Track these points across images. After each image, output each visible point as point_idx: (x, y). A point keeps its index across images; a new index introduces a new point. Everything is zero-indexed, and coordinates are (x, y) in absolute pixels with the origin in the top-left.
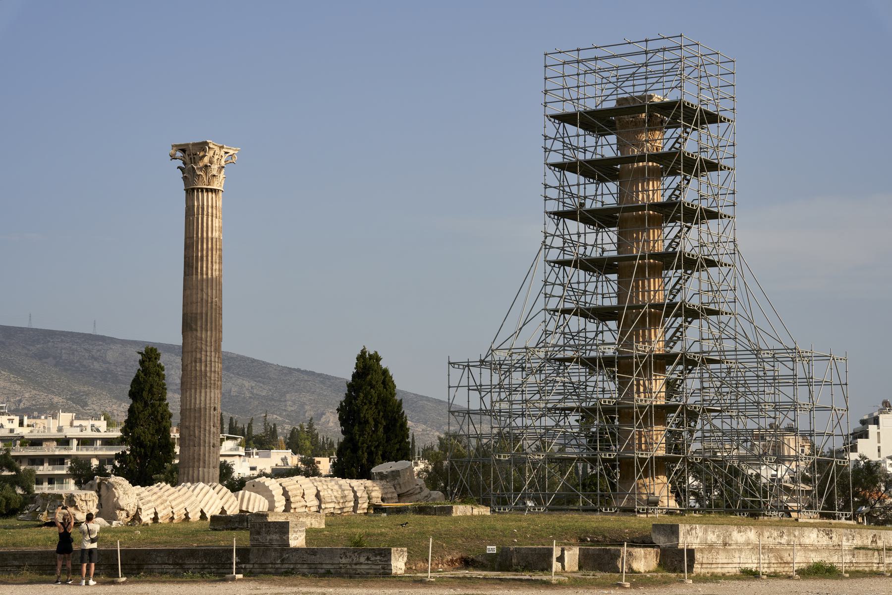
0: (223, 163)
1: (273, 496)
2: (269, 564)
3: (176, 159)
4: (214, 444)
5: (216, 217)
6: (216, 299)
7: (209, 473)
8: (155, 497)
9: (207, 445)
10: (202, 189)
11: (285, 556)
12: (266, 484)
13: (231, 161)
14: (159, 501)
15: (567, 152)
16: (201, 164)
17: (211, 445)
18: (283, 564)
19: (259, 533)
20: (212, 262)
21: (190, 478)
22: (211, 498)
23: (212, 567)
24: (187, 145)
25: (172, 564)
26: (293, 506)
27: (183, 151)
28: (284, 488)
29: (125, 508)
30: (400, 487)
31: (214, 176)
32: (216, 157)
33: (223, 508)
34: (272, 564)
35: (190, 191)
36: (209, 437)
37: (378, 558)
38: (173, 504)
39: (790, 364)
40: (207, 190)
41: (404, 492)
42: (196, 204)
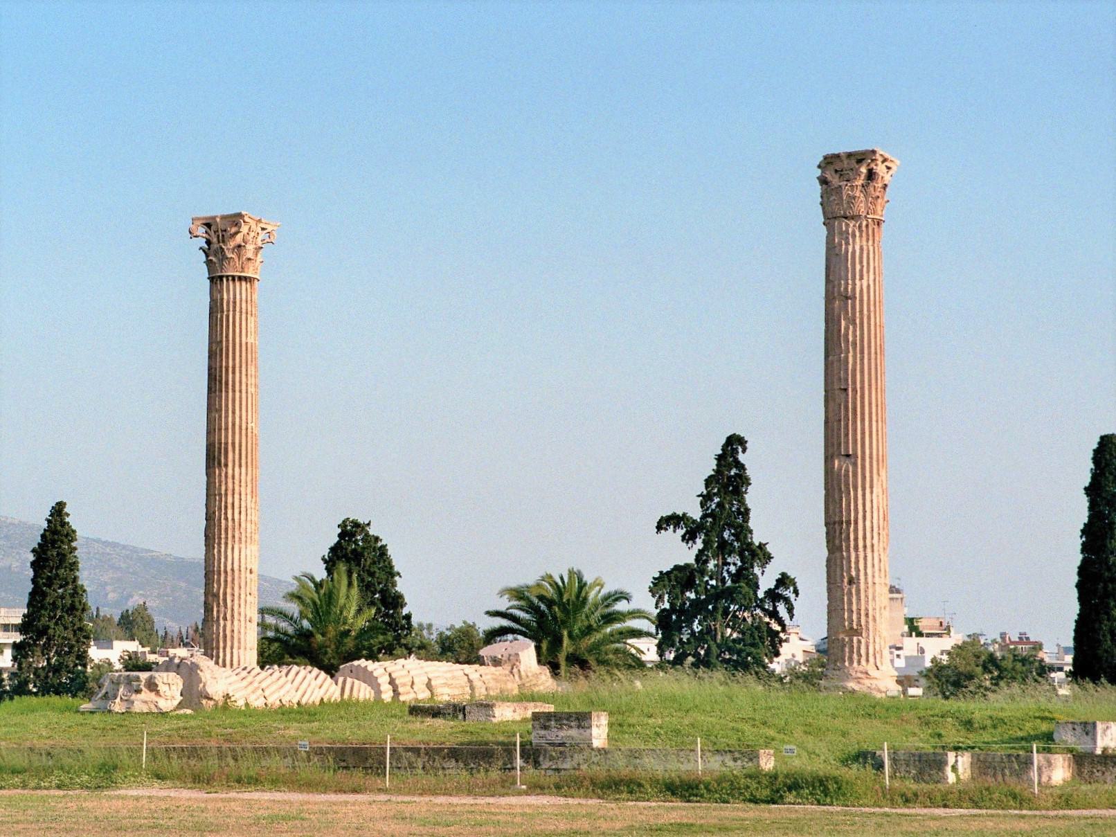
1: (379, 685)
4: (251, 618)
5: (252, 315)
6: (253, 424)
8: (245, 683)
9: (242, 619)
10: (233, 278)
12: (370, 669)
13: (269, 241)
14: (251, 688)
16: (232, 244)
17: (248, 619)
20: (247, 375)
21: (221, 661)
22: (309, 685)
24: (214, 218)
27: (208, 225)
28: (390, 675)
31: (249, 259)
32: (252, 234)
35: (215, 280)
38: (267, 693)
40: (240, 278)
42: (225, 297)
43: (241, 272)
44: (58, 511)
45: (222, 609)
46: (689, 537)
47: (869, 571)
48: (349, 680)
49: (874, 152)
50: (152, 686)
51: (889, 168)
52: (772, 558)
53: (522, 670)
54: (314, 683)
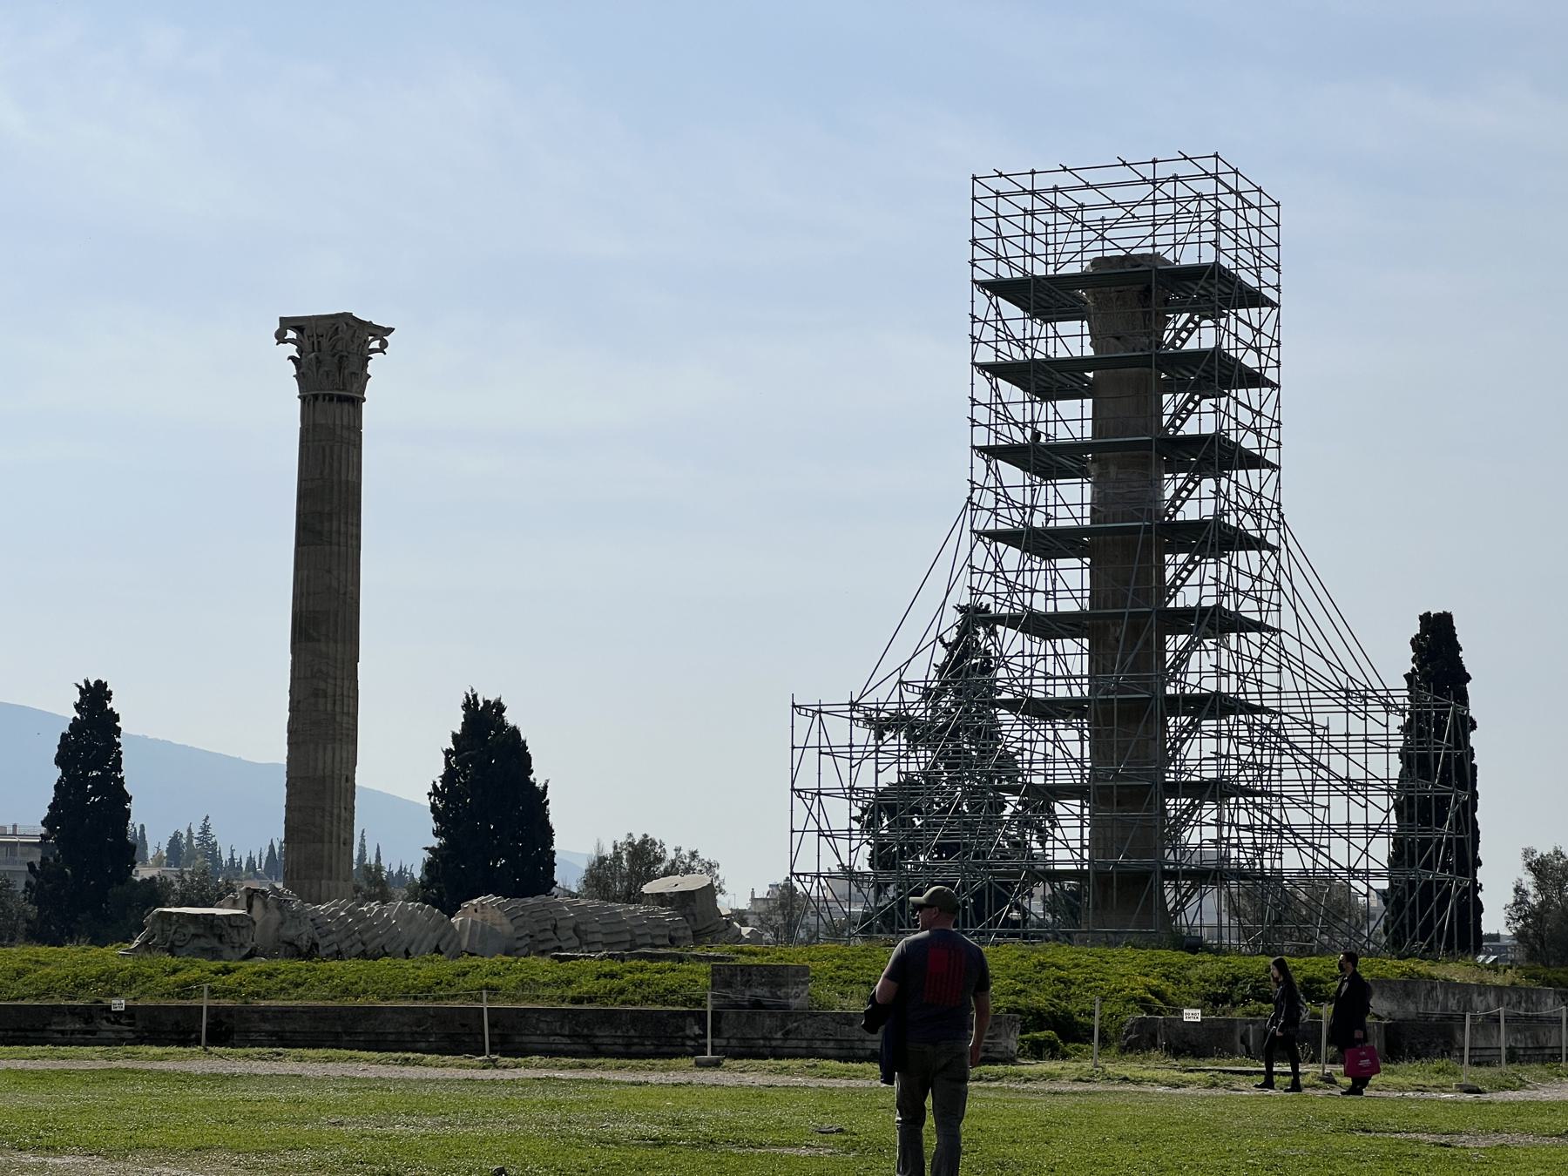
2: (759, 1039)
3: (285, 342)
4: (345, 839)
7: (337, 889)
11: (792, 1025)
15: (1003, 346)
18: (786, 1039)
19: (729, 985)
20: (346, 523)
23: (646, 1043)
25: (569, 1036)
29: (296, 943)
30: (695, 920)
33: (438, 946)
34: (764, 1038)
36: (339, 827)
39: (1382, 717)
40: (341, 399)
41: (700, 928)
43: (343, 390)
44: (95, 697)
46: (914, 742)
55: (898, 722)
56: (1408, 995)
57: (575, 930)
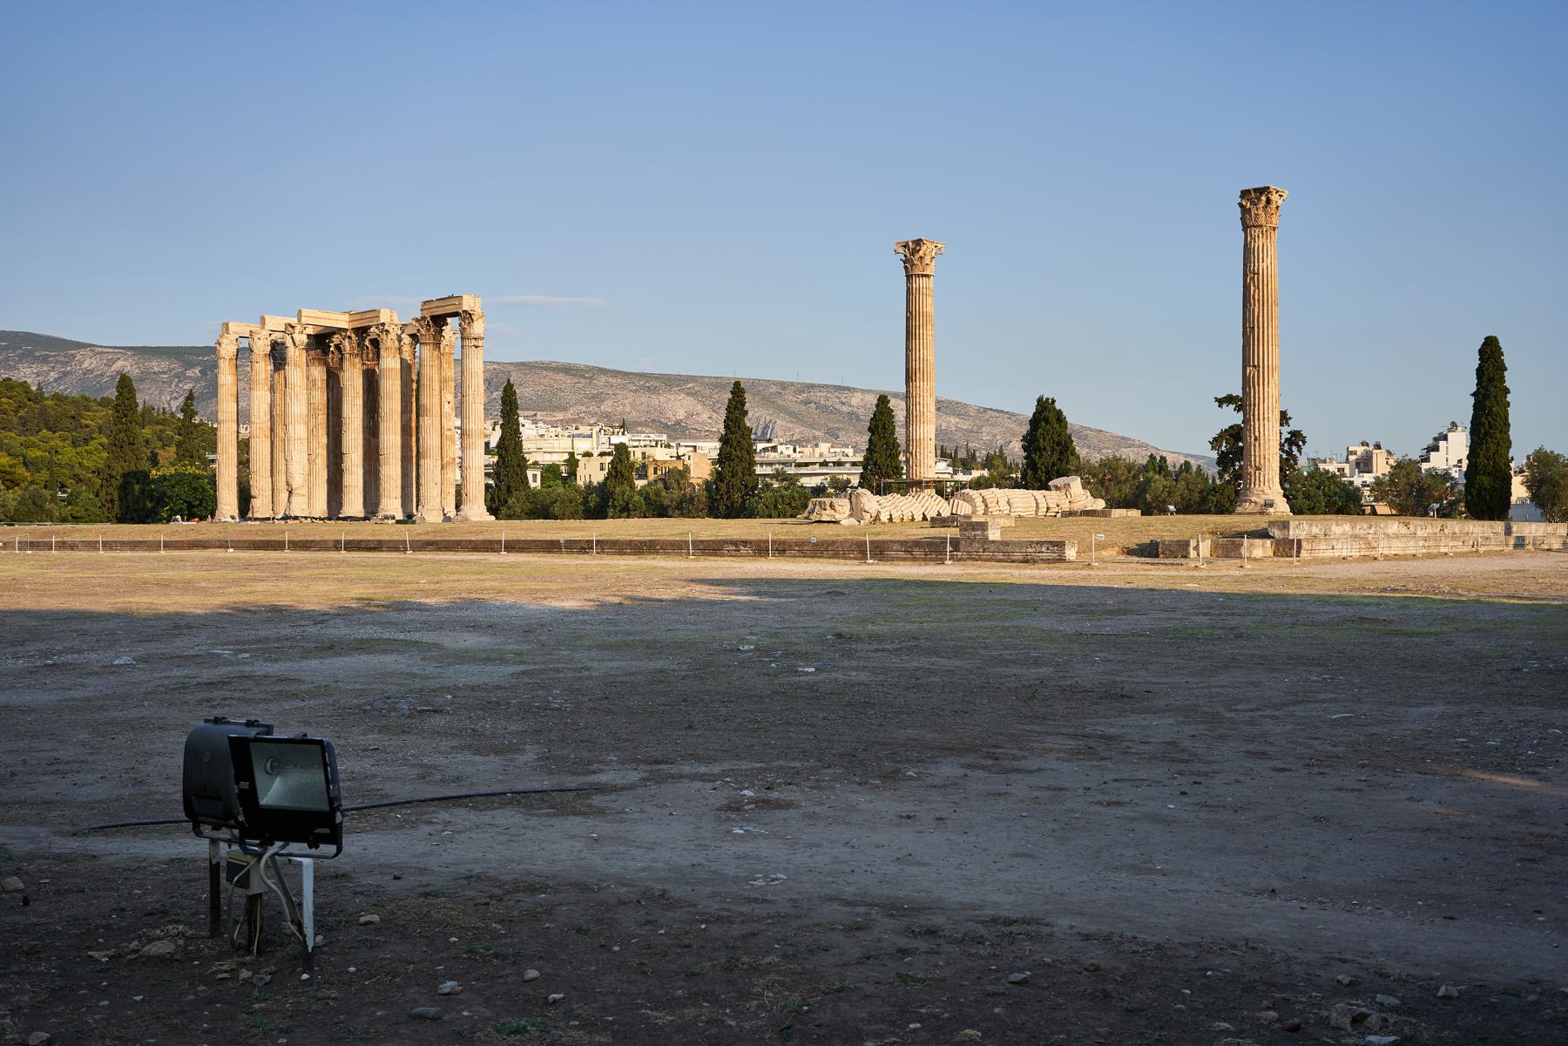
0: (934, 255)
14: (893, 506)
16: (917, 256)
19: (966, 530)
26: (990, 510)
28: (983, 497)
32: (929, 250)
35: (909, 277)
37: (1056, 548)
40: (923, 276)
42: (914, 286)
45: (915, 460)
47: (1266, 433)
48: (956, 501)
49: (1268, 188)
50: (832, 506)
51: (1280, 196)
52: (1290, 418)
53: (1072, 492)
54: (933, 503)
55: (1229, 399)
56: (1285, 528)
57: (1008, 503)
